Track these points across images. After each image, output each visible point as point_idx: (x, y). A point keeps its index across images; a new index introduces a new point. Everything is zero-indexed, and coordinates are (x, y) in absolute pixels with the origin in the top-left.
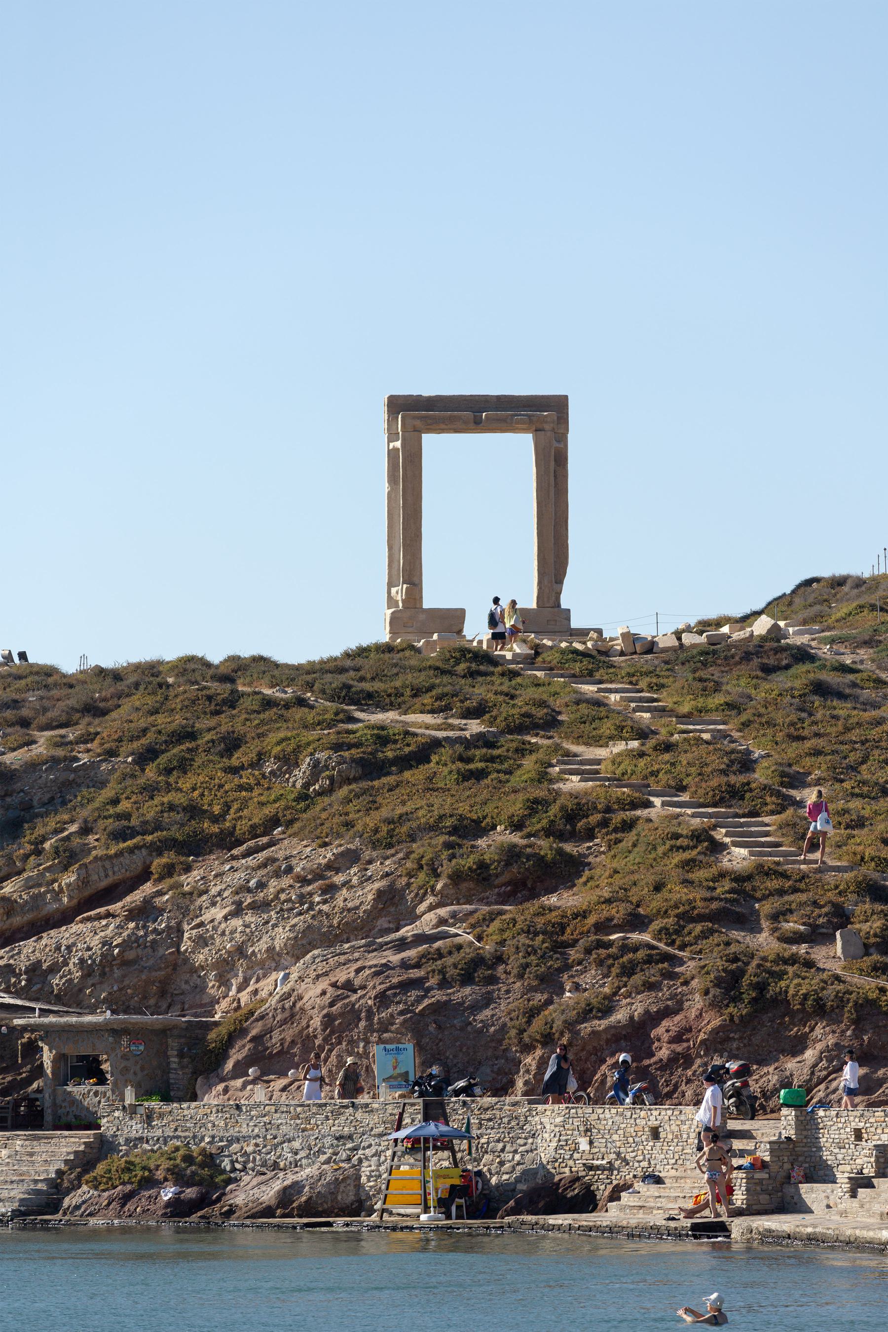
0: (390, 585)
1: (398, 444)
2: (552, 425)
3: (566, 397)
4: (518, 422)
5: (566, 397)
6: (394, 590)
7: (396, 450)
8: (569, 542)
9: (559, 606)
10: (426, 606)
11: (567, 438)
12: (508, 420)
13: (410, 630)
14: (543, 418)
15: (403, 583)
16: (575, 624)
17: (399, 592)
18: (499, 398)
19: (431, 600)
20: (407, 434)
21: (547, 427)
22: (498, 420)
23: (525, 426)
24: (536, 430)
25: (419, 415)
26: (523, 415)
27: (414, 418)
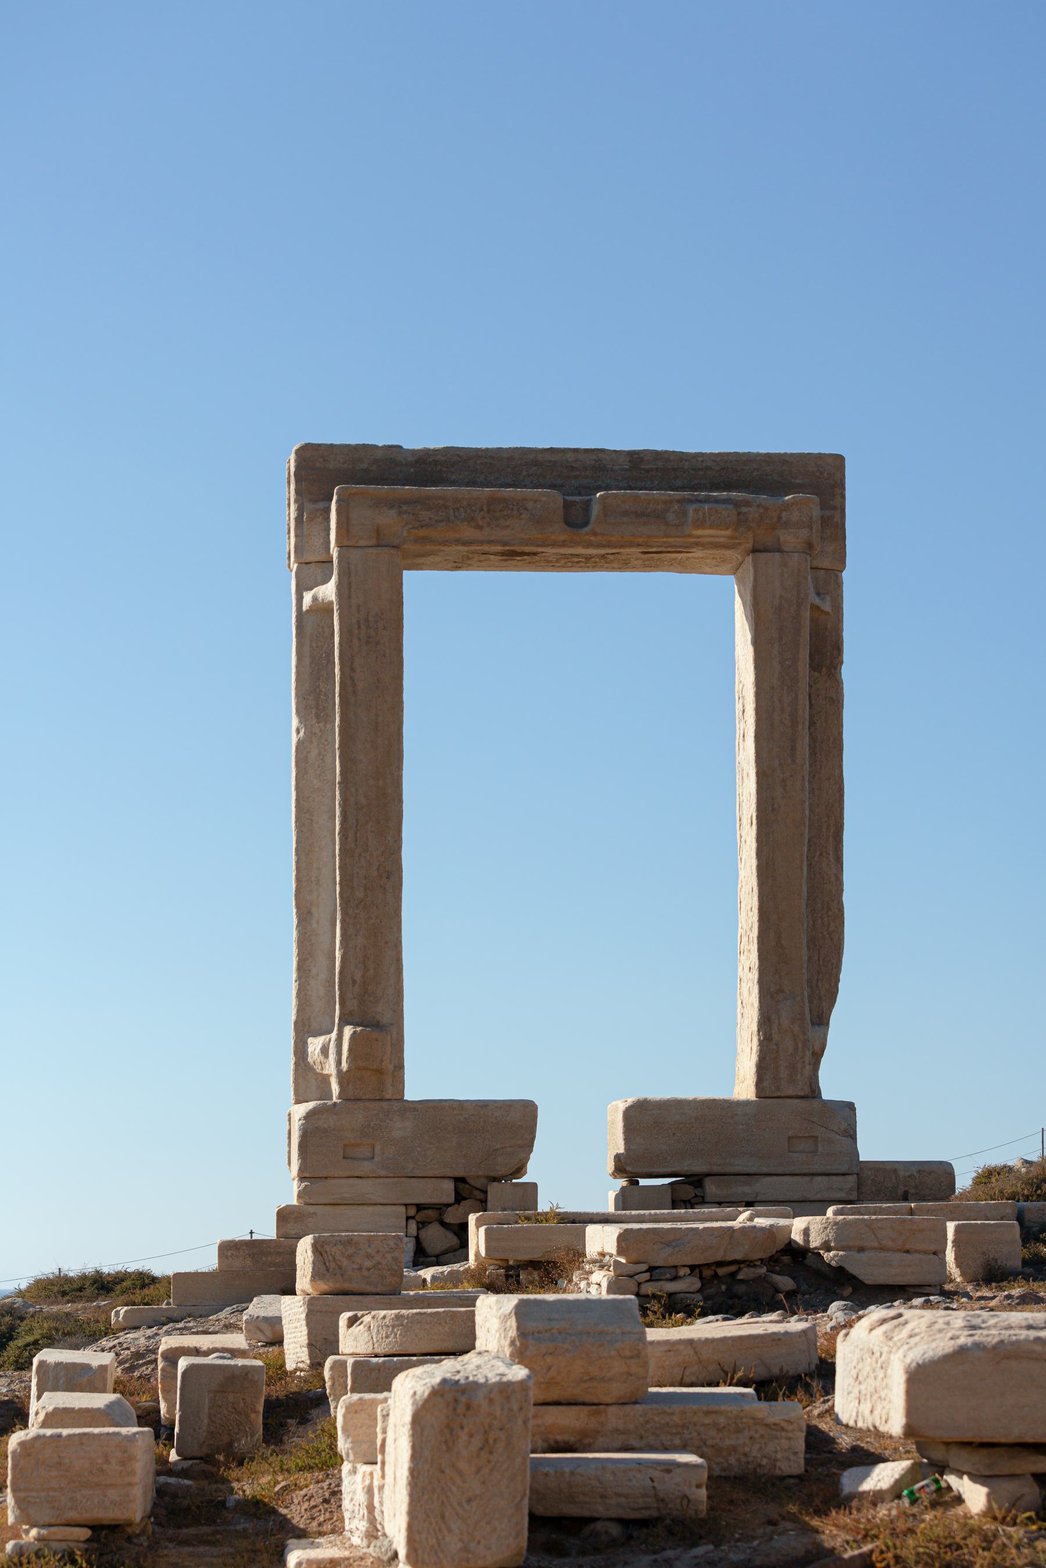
0: (304, 1029)
1: (328, 591)
2: (804, 534)
3: (839, 461)
4: (699, 524)
5: (839, 461)
6: (315, 1044)
7: (322, 609)
8: (847, 898)
9: (814, 1092)
10: (413, 1092)
11: (839, 585)
12: (671, 517)
13: (366, 1167)
14: (771, 519)
15: (344, 1021)
16: (874, 1145)
17: (331, 1052)
18: (636, 458)
19: (430, 1074)
20: (355, 555)
21: (790, 539)
22: (637, 515)
23: (722, 534)
24: (754, 551)
25: (395, 509)
26: (716, 501)
27: (379, 503)
